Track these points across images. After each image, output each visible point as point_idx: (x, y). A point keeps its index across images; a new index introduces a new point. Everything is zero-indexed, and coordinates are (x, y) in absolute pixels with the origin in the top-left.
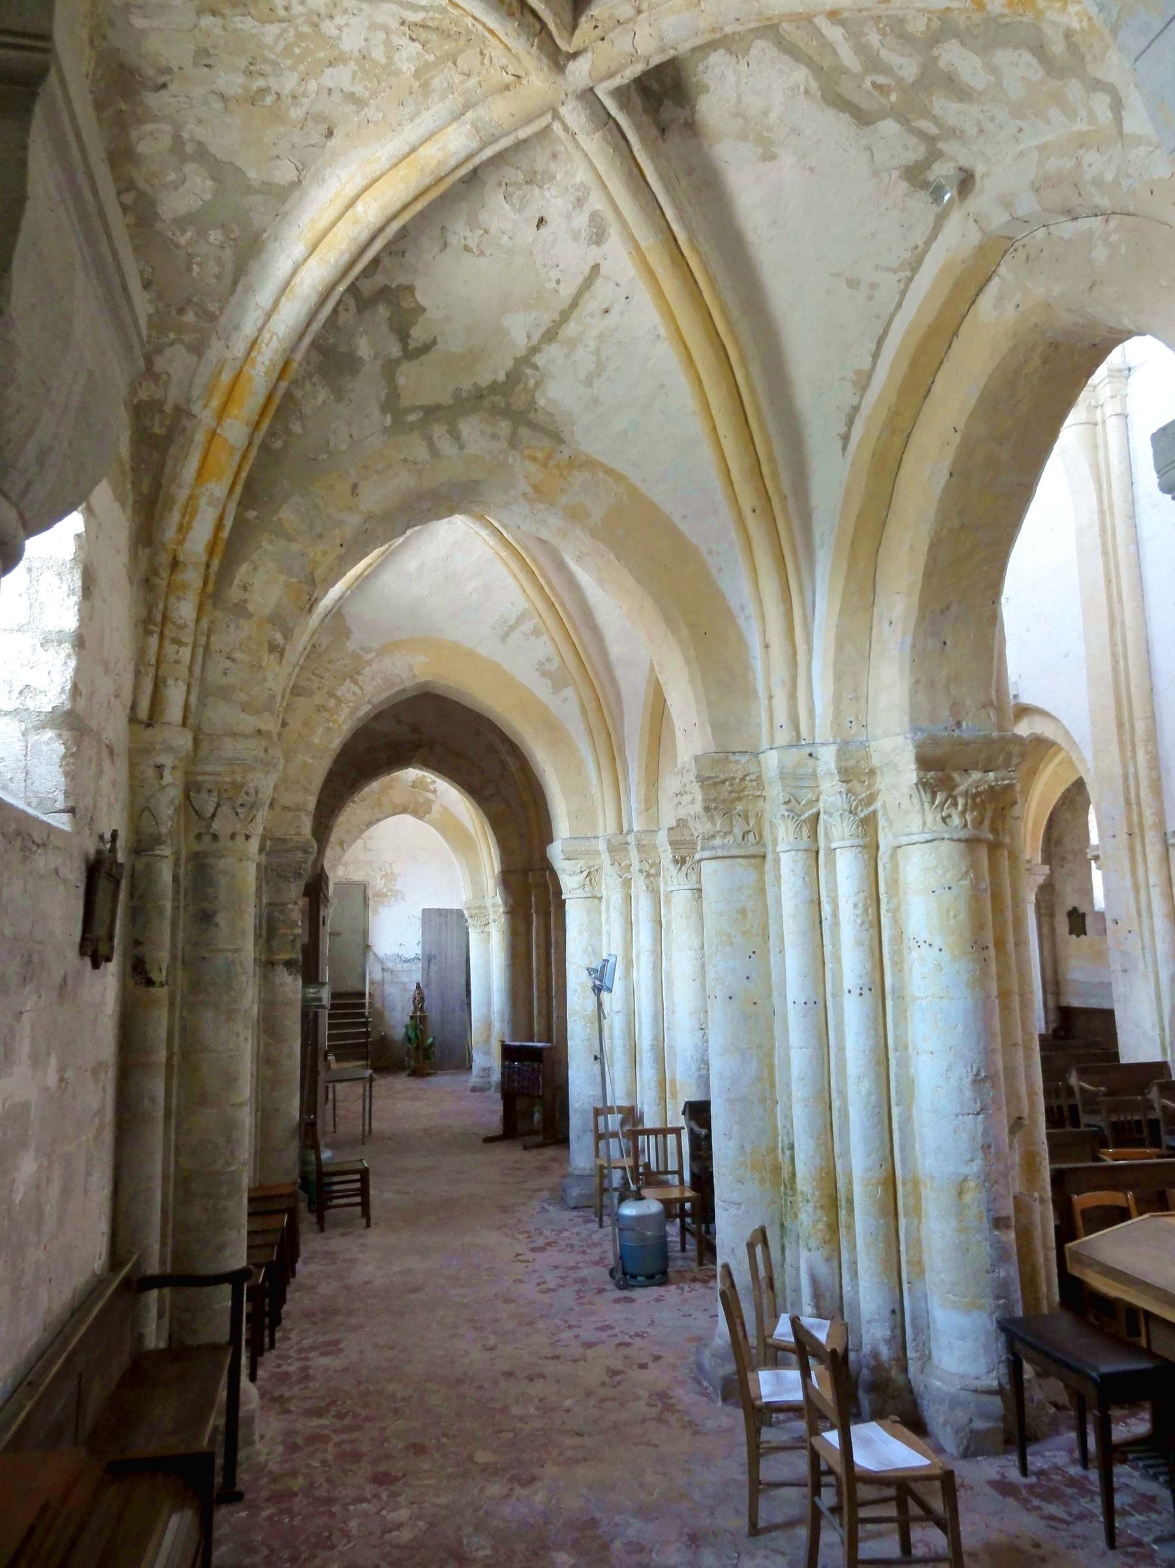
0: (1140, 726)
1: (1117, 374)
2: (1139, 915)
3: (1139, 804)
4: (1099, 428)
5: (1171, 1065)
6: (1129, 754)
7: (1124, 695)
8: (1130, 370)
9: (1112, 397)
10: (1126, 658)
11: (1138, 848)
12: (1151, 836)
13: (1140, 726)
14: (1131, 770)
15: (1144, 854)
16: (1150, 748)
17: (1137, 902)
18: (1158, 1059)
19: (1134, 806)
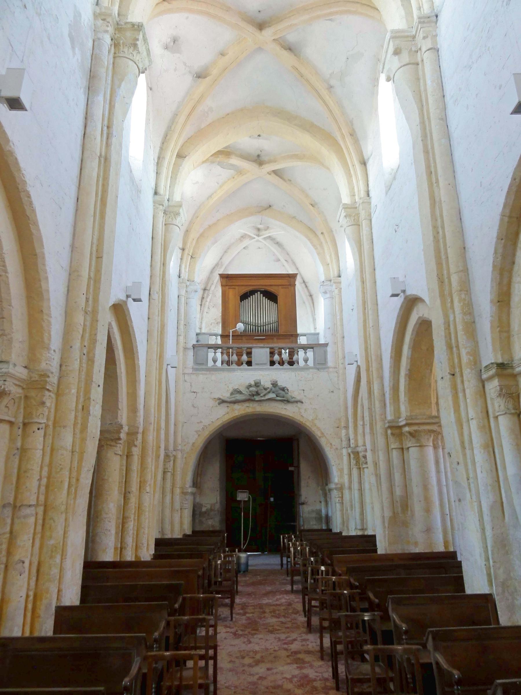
0: (455, 279)
1: (426, 20)
2: (463, 447)
3: (458, 347)
4: (420, 66)
5: (497, 598)
6: (449, 305)
7: (443, 257)
8: (437, 16)
9: (424, 38)
10: (443, 228)
11: (460, 386)
12: (468, 374)
13: (455, 279)
14: (451, 319)
15: (464, 390)
16: (463, 296)
17: (461, 435)
18: (487, 592)
19: (455, 349)
